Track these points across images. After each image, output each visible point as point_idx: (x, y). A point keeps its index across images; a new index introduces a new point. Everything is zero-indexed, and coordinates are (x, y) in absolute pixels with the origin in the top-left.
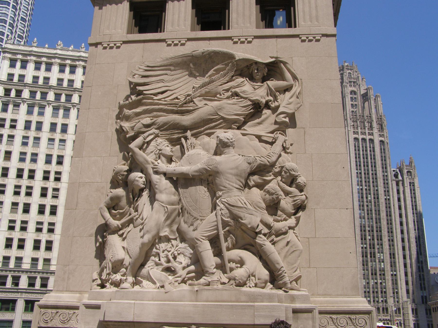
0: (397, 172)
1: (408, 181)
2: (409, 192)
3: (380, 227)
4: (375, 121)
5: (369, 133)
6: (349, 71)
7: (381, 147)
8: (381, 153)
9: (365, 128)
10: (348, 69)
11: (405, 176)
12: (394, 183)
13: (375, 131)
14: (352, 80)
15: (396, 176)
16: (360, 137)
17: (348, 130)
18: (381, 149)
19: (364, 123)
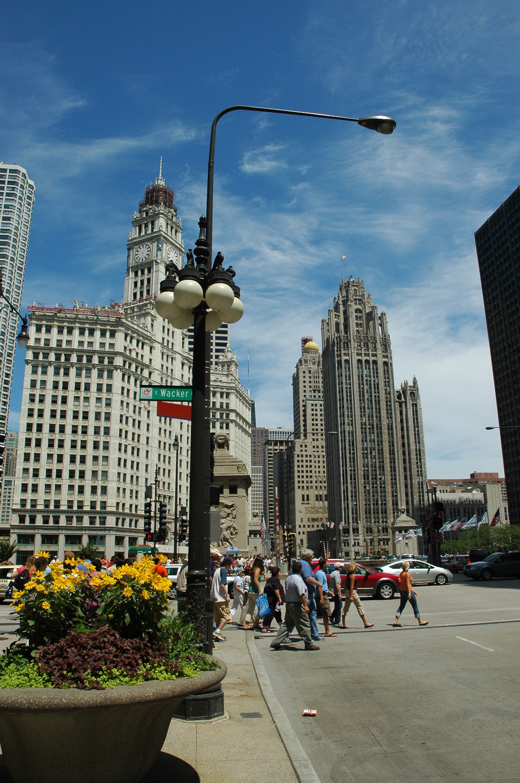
0: (400, 394)
1: (411, 402)
2: (412, 414)
3: (382, 450)
4: (378, 341)
5: (372, 354)
6: (355, 288)
7: (384, 368)
8: (385, 374)
9: (368, 350)
10: (354, 286)
11: (408, 397)
12: (397, 404)
13: (379, 352)
15: (399, 397)
16: (364, 358)
17: (351, 352)
18: (384, 371)
19: (367, 344)
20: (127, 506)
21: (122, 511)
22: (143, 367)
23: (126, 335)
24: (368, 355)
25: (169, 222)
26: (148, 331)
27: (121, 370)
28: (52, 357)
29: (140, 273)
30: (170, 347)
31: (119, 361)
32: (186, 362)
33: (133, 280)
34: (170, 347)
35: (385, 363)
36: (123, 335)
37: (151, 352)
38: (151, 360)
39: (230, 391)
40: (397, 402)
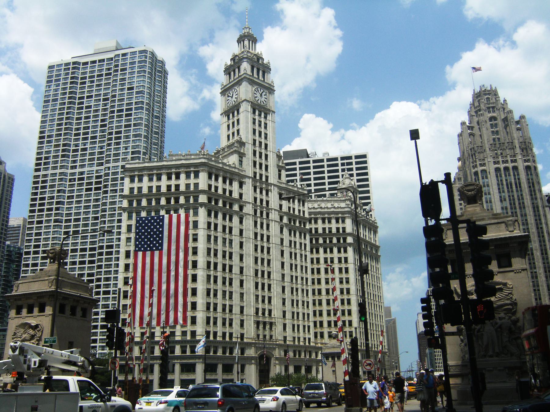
14: (491, 105)
16: (502, 166)
20: (219, 334)
21: (221, 339)
24: (507, 162)
25: (255, 64)
26: (235, 168)
28: (144, 203)
29: (231, 115)
30: (264, 179)
31: (203, 199)
33: (227, 124)
34: (264, 179)
35: (528, 168)
37: (241, 186)
38: (241, 195)
40: (547, 206)
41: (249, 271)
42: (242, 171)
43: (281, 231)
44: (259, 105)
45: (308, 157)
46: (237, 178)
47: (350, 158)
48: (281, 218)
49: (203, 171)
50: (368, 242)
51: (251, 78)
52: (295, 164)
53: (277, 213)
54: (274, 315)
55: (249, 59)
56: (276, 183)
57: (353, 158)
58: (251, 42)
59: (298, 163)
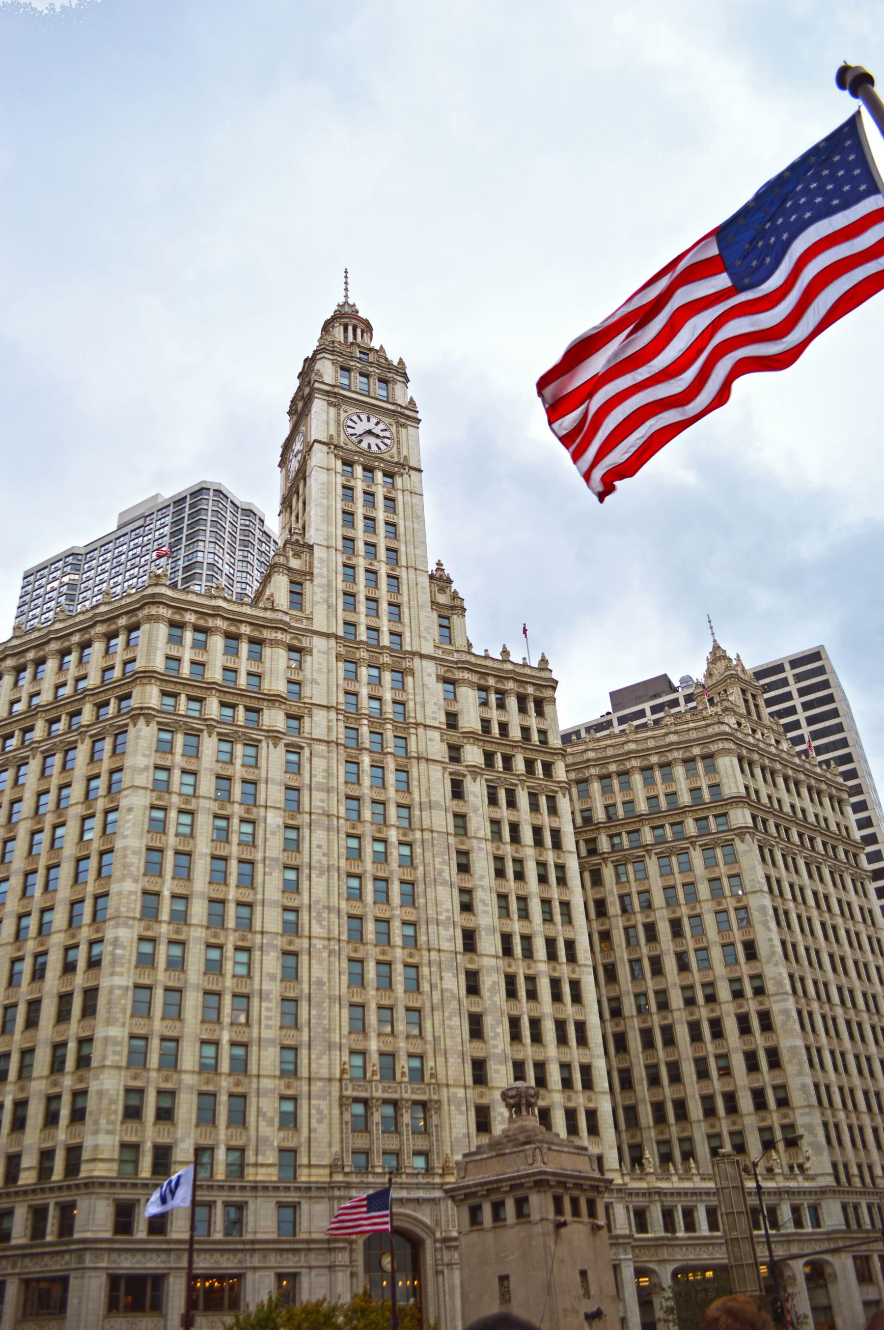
22: (254, 704)
23: (176, 625)
26: (273, 610)
27: (149, 718)
32: (459, 675)
36: (163, 630)
39: (713, 748)
41: (322, 927)
42: (299, 620)
43: (458, 791)
44: (361, 453)
45: (674, 690)
46: (279, 635)
47: (778, 668)
48: (455, 753)
49: (151, 618)
50: (816, 829)
51: (336, 390)
52: (641, 714)
53: (436, 735)
54: (433, 1075)
55: (332, 353)
56: (428, 648)
57: (787, 667)
58: (350, 328)
59: (648, 712)
